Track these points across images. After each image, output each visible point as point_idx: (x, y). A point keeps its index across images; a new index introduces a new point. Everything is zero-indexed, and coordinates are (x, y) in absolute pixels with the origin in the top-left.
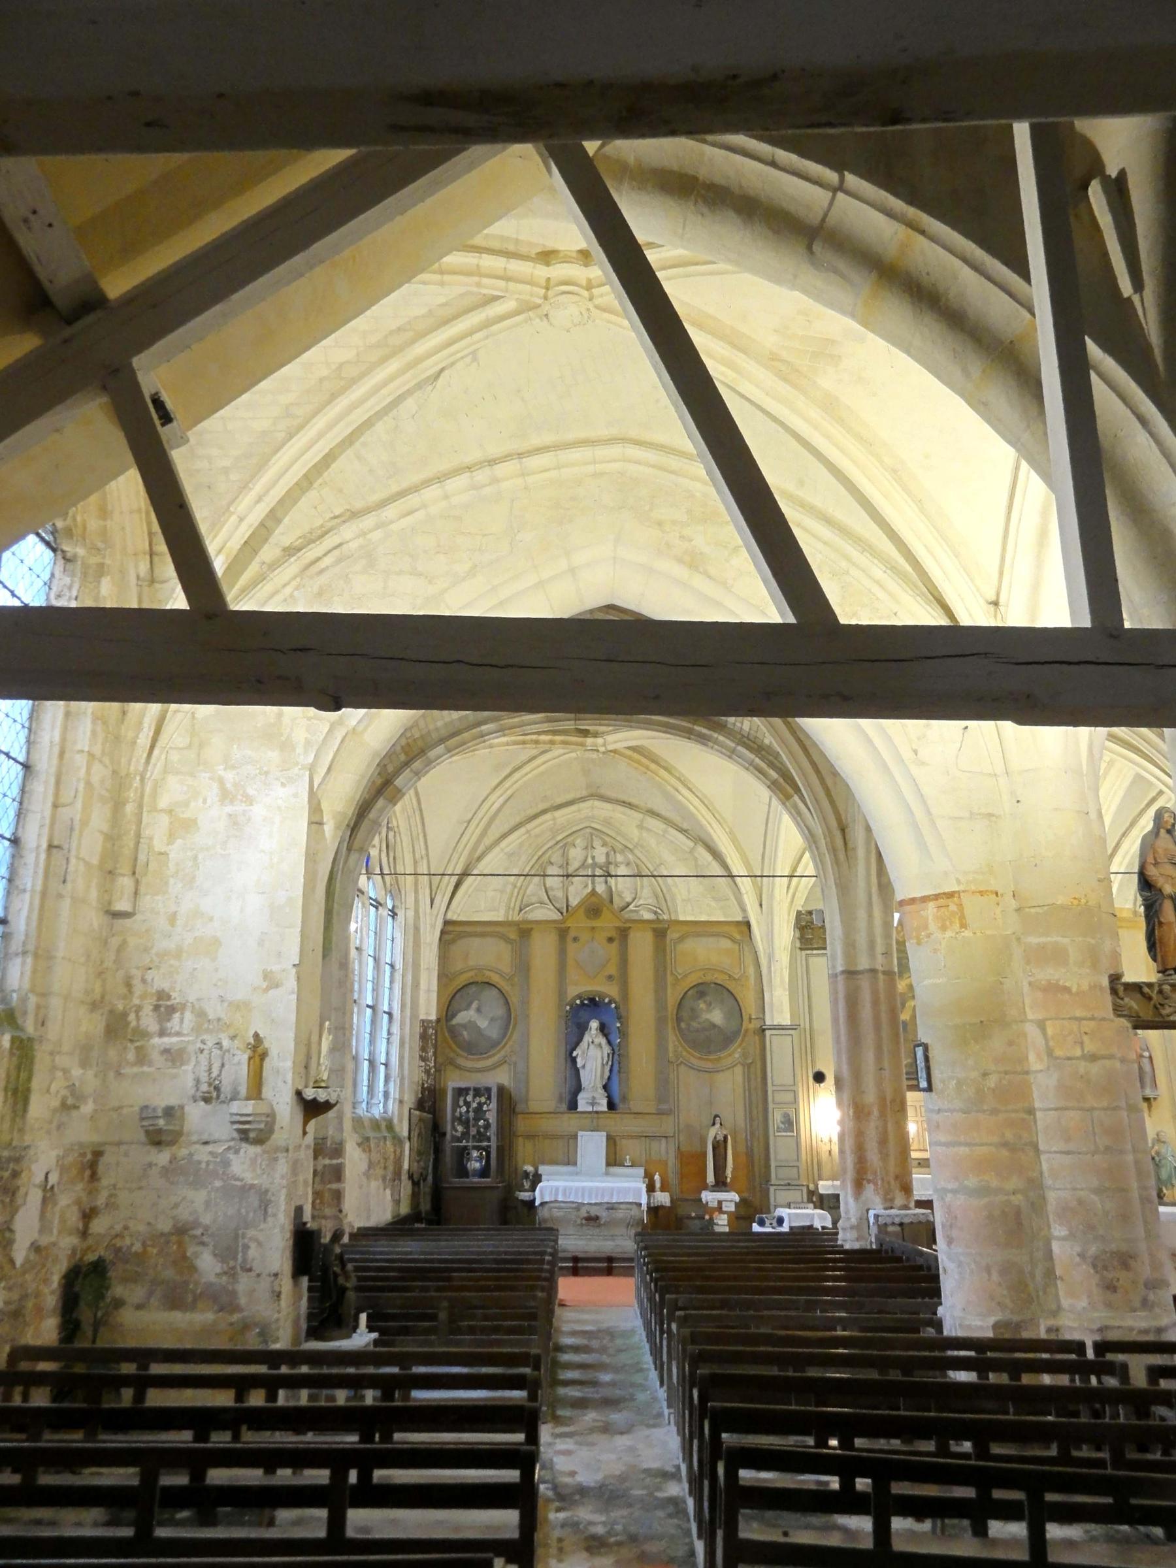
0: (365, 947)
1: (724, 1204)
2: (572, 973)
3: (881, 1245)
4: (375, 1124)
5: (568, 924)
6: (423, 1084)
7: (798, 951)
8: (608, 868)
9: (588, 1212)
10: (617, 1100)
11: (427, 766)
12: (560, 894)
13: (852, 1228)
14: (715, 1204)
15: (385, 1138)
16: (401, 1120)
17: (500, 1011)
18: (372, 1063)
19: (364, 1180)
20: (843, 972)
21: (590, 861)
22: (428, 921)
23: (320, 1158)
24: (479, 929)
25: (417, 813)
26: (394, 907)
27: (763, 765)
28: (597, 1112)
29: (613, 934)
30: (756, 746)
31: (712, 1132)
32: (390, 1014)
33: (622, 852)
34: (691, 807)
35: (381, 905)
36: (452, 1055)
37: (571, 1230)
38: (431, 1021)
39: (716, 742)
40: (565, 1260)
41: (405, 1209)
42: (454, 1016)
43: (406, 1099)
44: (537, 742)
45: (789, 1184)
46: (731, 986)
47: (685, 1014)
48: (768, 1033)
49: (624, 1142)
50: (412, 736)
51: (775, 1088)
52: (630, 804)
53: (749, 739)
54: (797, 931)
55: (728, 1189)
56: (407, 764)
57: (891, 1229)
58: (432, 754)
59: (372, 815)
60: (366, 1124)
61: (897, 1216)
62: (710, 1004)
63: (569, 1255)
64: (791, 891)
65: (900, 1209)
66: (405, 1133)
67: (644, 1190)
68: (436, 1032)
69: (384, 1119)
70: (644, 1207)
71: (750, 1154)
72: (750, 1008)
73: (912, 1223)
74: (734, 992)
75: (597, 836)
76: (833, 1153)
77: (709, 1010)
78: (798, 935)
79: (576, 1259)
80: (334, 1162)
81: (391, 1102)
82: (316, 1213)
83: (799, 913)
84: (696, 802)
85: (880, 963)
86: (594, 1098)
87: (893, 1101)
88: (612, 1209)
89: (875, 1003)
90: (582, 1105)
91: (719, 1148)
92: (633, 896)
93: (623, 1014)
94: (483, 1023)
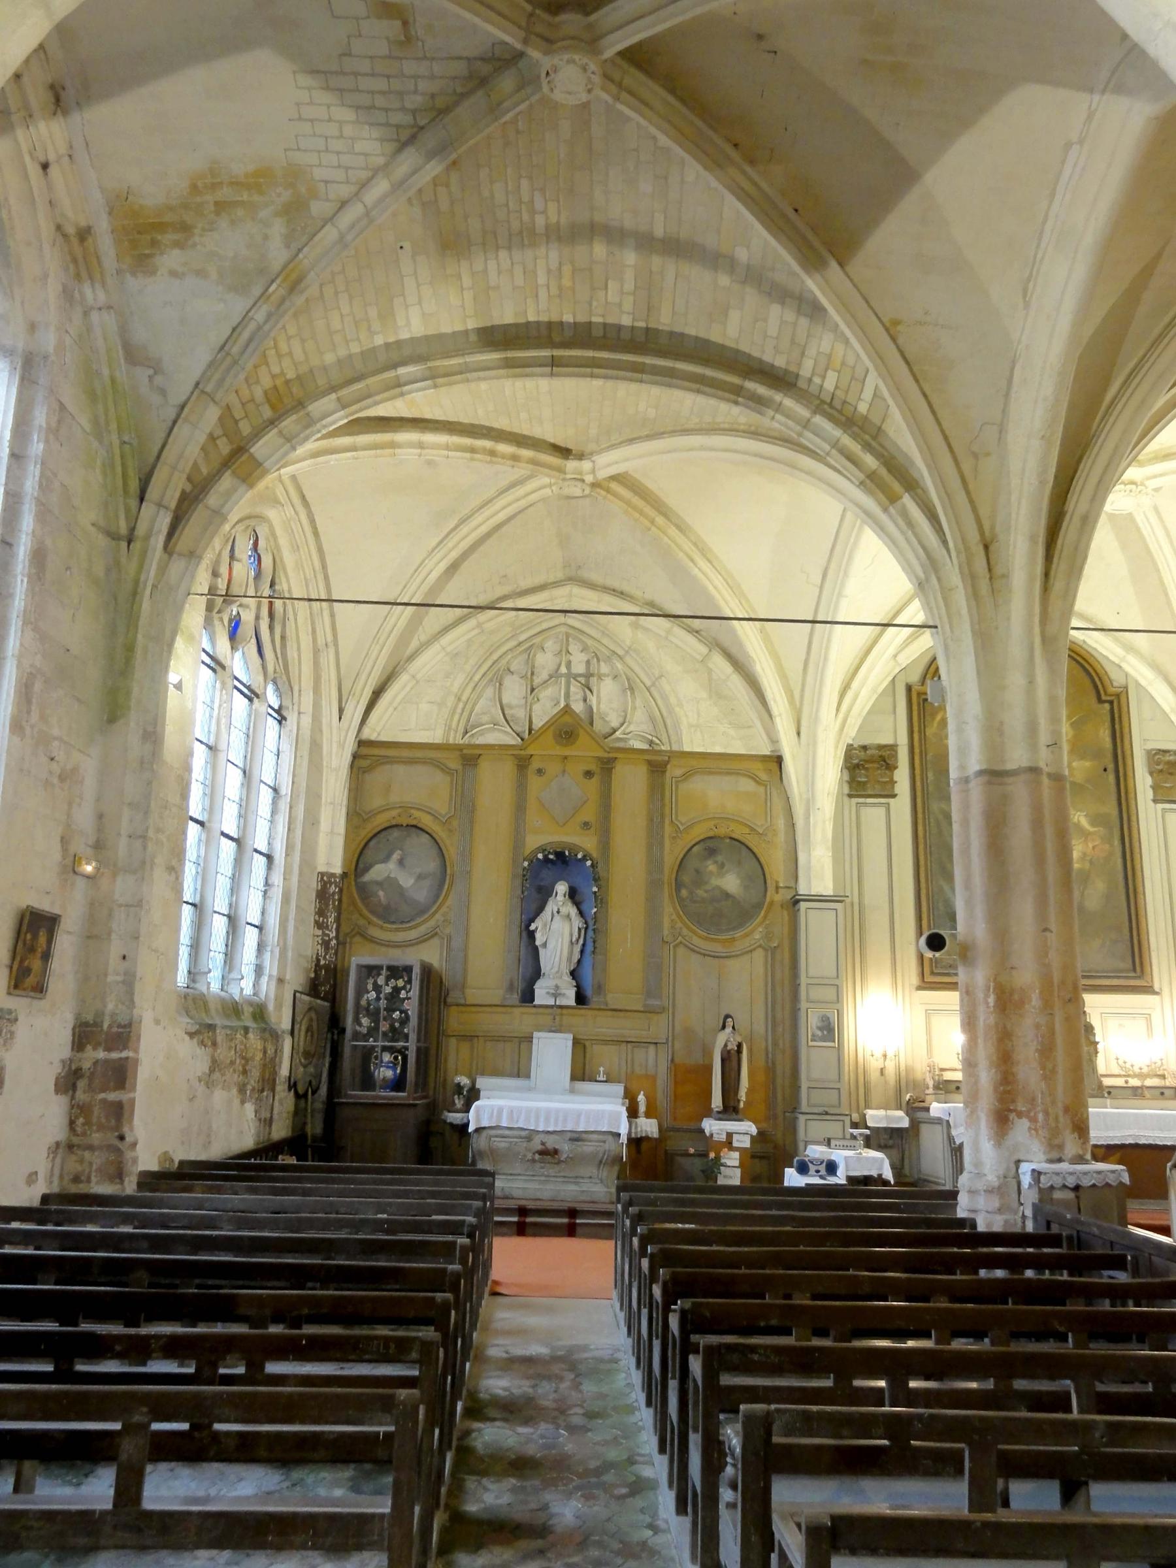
0: (222, 746)
1: (735, 1137)
2: (533, 818)
3: (1048, 1224)
4: (233, 1009)
5: (530, 751)
6: (318, 960)
7: (846, 799)
8: (588, 681)
9: (543, 1144)
10: (589, 992)
11: (307, 427)
12: (521, 714)
13: (989, 1191)
14: (723, 1137)
15: (246, 1030)
16: (279, 1006)
17: (432, 866)
18: (233, 920)
19: (201, 1089)
20: (981, 773)
21: (563, 670)
22: (335, 739)
23: (89, 1047)
24: (405, 753)
25: (320, 577)
26: (280, 707)
27: (855, 447)
28: (561, 1007)
29: (592, 767)
30: (843, 419)
31: (722, 1038)
32: (269, 858)
33: (608, 660)
34: (711, 588)
35: (257, 696)
36: (362, 922)
37: (518, 1168)
38: (333, 875)
39: (779, 408)
40: (507, 1211)
41: (280, 1131)
42: (367, 869)
43: (288, 977)
44: (492, 453)
45: (827, 1113)
46: (752, 841)
47: (686, 878)
48: (803, 905)
49: (597, 1049)
50: (283, 373)
51: (810, 981)
52: (622, 593)
53: (831, 405)
54: (846, 772)
55: (740, 1116)
56: (272, 423)
57: (1058, 1195)
58: (315, 408)
59: (212, 500)
60: (212, 1006)
61: (1071, 1174)
62: (722, 866)
63: (512, 1204)
64: (841, 716)
66: (286, 1024)
67: (625, 1114)
68: (341, 891)
69: (251, 1003)
70: (624, 1139)
71: (771, 1070)
72: (777, 870)
73: (1094, 1186)
74: (755, 850)
75: (575, 638)
77: (721, 874)
78: (846, 777)
79: (523, 1211)
80: (115, 1055)
81: (264, 980)
82: (75, 1140)
83: (850, 748)
84: (718, 581)
85: (1043, 759)
86: (557, 987)
87: (1063, 982)
88: (577, 1140)
89: (1037, 824)
90: (542, 995)
91: (731, 1059)
92: (621, 720)
93: (602, 874)
94: (407, 881)
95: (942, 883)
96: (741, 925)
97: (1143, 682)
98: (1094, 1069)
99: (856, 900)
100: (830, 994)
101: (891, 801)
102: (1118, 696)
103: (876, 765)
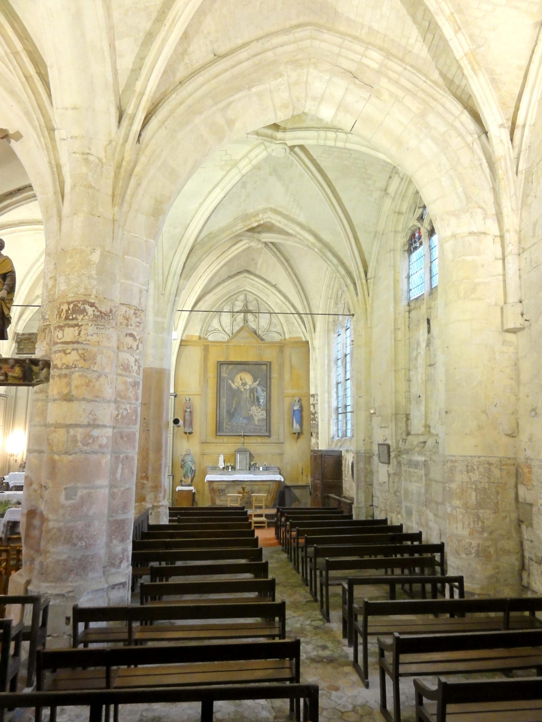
54: (17, 344)
78: (17, 346)
99: (14, 395)
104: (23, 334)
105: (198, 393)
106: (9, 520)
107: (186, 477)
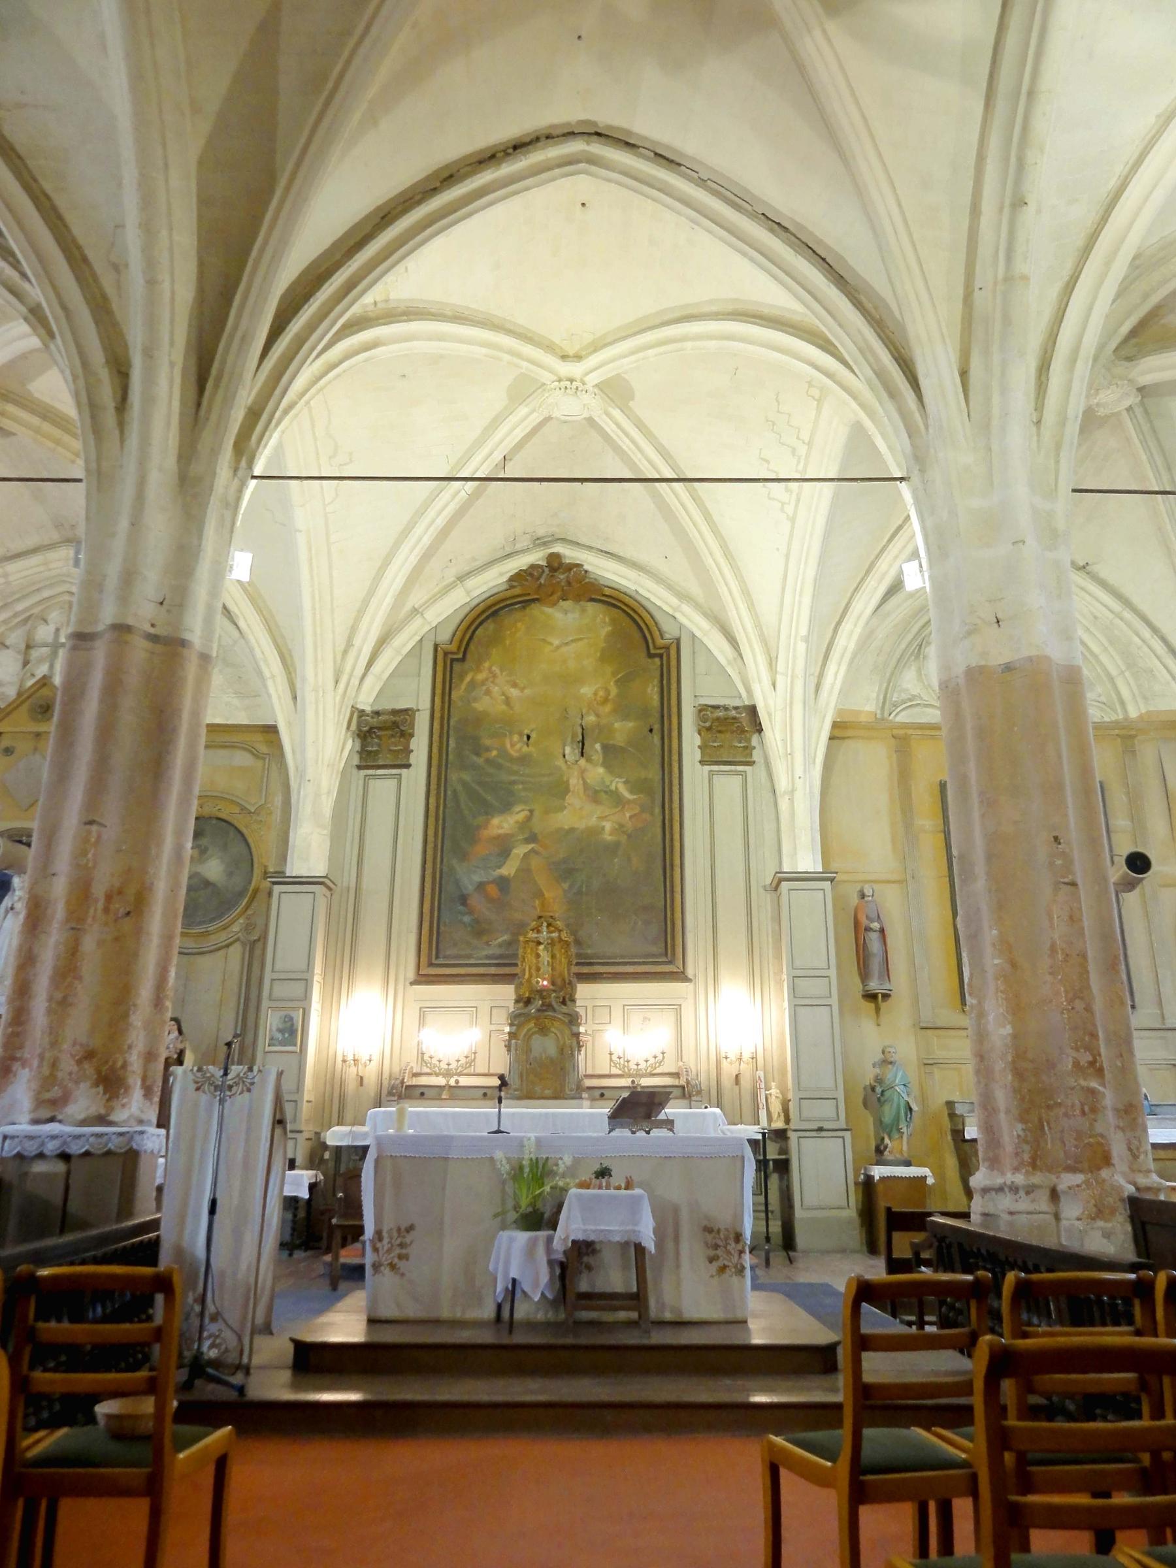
7: (355, 771)
46: (240, 821)
51: (275, 976)
57: (39, 1167)
65: (83, 1123)
72: (265, 854)
73: (87, 1154)
76: (365, 1081)
78: (358, 747)
95: (454, 862)
96: (220, 916)
97: (698, 634)
98: (575, 1067)
99: (353, 885)
100: (297, 989)
101: (404, 771)
102: (667, 648)
103: (390, 732)
104: (377, 713)
105: (895, 877)
106: (580, 1237)
107: (896, 1136)
